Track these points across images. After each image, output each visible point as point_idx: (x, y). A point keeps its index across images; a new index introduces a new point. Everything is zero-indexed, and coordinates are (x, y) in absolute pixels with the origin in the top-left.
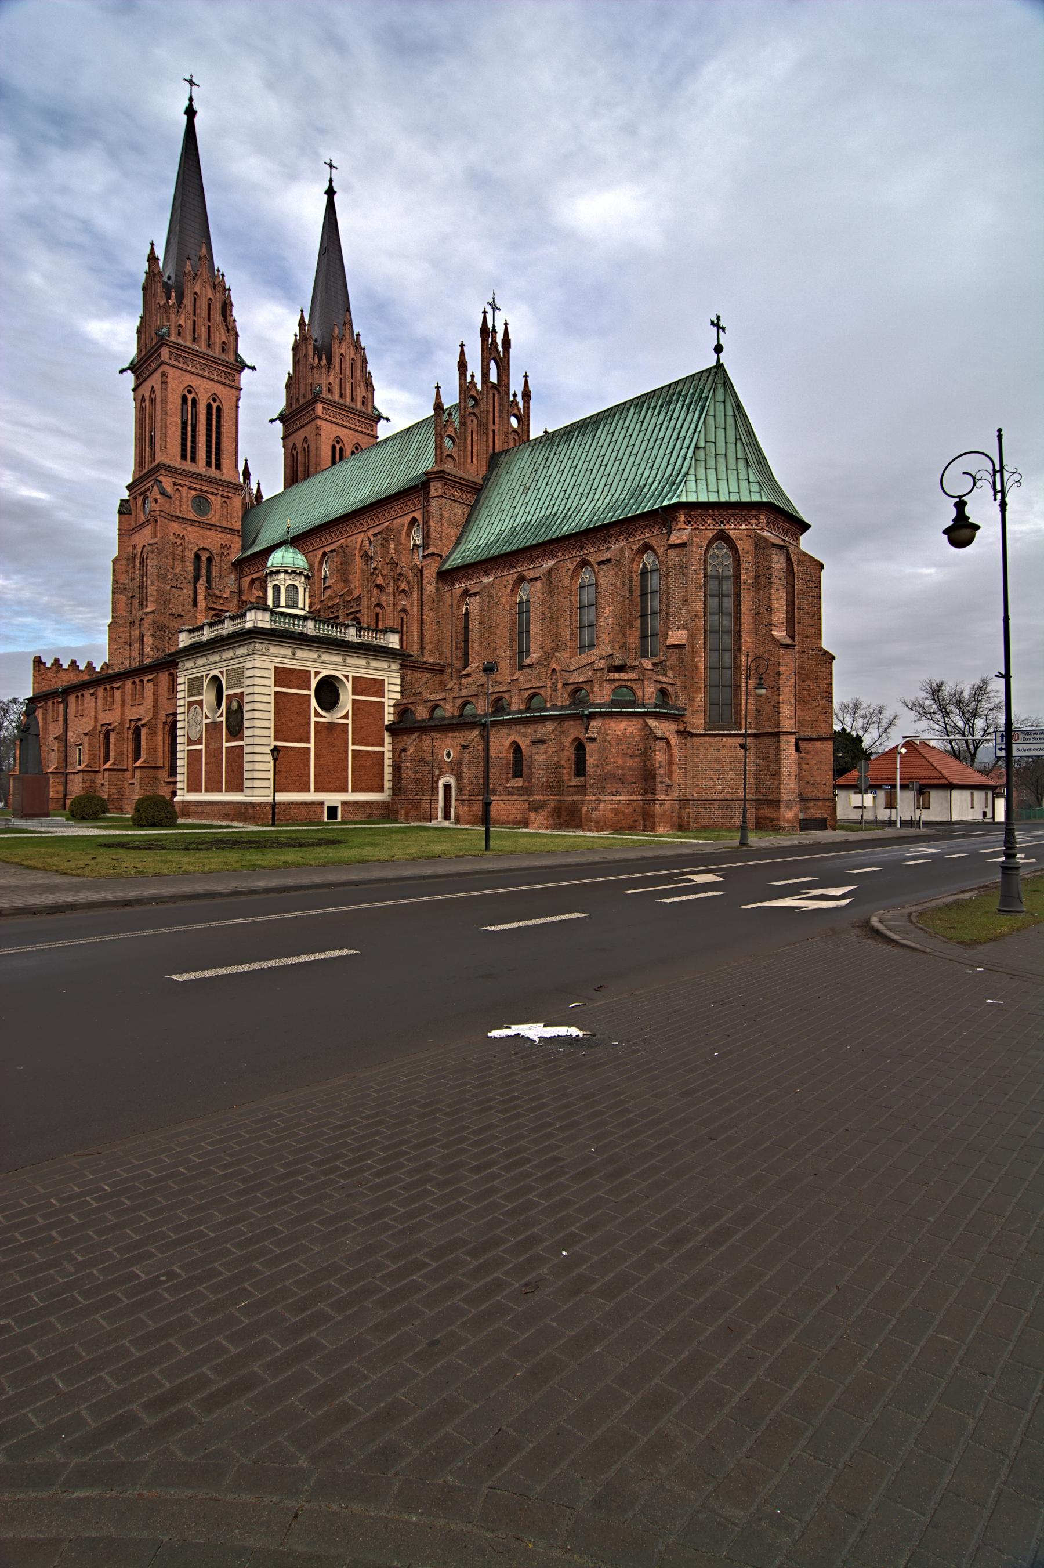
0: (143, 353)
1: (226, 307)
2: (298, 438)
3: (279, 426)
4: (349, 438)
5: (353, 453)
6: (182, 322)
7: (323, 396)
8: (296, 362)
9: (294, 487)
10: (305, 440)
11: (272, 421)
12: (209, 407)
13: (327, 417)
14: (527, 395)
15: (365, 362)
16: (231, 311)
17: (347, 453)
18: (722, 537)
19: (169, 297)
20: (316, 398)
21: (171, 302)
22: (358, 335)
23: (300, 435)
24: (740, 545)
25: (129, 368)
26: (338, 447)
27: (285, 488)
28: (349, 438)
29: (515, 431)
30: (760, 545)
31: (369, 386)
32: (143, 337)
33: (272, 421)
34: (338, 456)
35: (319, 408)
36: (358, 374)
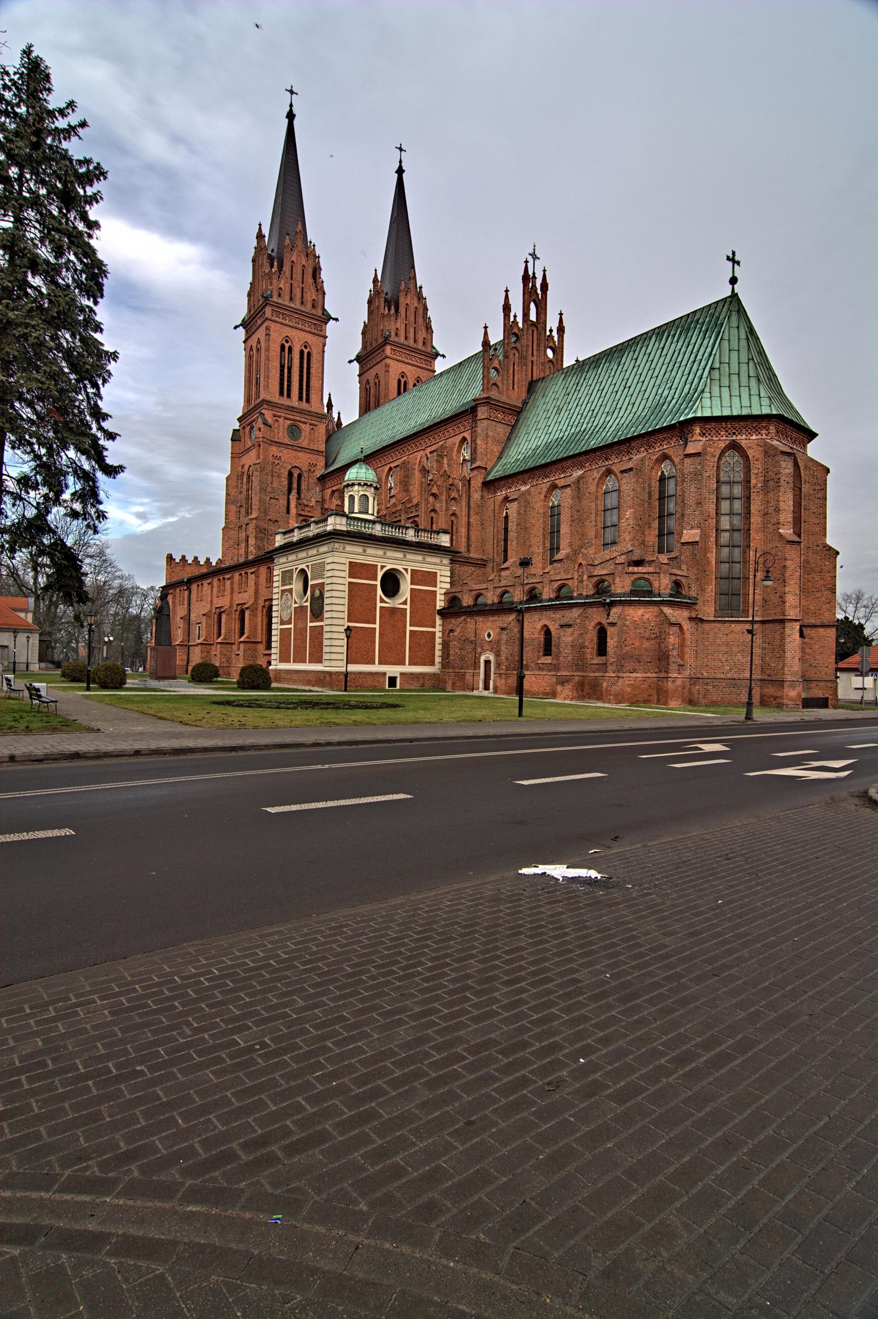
1: (316, 271)
4: (411, 373)
5: (415, 385)
8: (370, 313)
9: (367, 415)
10: (377, 376)
11: (350, 362)
12: (302, 352)
14: (561, 330)
15: (426, 309)
16: (320, 274)
17: (410, 385)
18: (734, 446)
19: (272, 266)
20: (386, 341)
21: (274, 270)
22: (421, 287)
24: (750, 453)
25: (241, 325)
26: (403, 381)
28: (411, 373)
29: (550, 361)
30: (769, 452)
31: (429, 329)
33: (350, 362)
34: (402, 388)
35: (388, 349)
36: (420, 320)
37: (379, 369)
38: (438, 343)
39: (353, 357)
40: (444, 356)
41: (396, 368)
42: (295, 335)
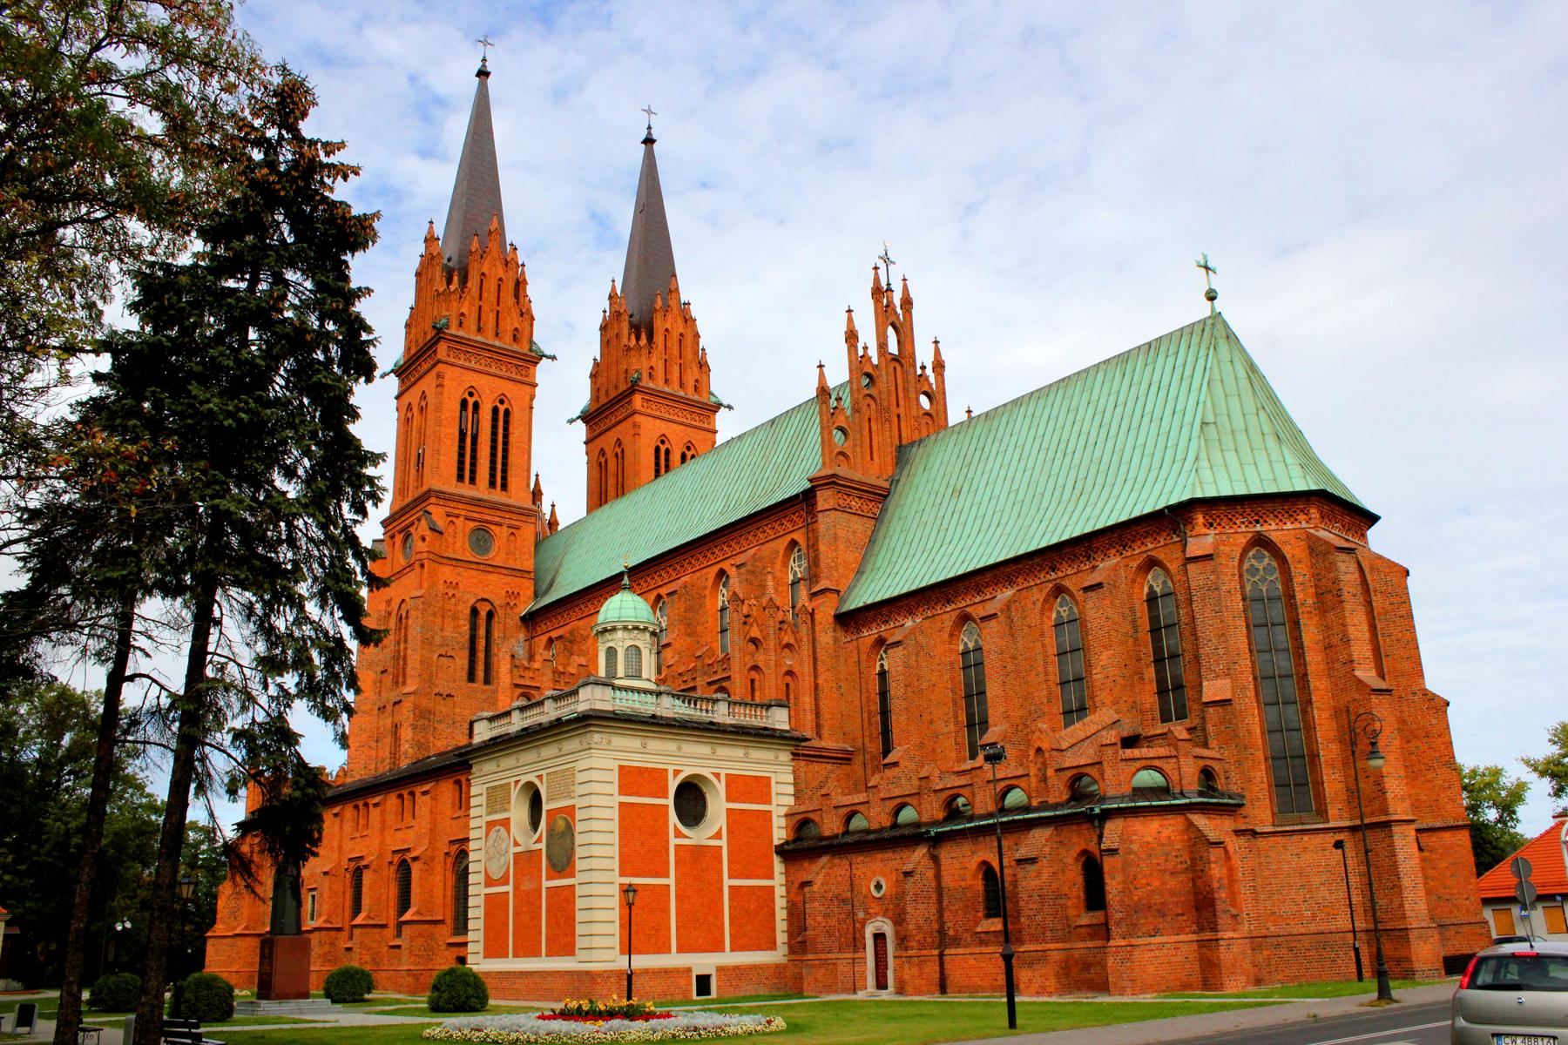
0: (413, 352)
1: (520, 284)
2: (608, 441)
3: (581, 429)
5: (684, 458)
6: (464, 310)
8: (606, 344)
9: (606, 508)
10: (619, 443)
11: (571, 421)
13: (649, 411)
14: (939, 366)
16: (525, 289)
18: (1261, 541)
19: (449, 282)
20: (634, 388)
21: (452, 288)
23: (609, 439)
24: (1288, 551)
25: (392, 371)
27: (590, 510)
28: (678, 437)
29: (927, 414)
30: (1317, 550)
32: (414, 331)
33: (571, 421)
34: (662, 464)
35: (638, 400)
37: (622, 431)
39: (578, 413)
42: (480, 382)
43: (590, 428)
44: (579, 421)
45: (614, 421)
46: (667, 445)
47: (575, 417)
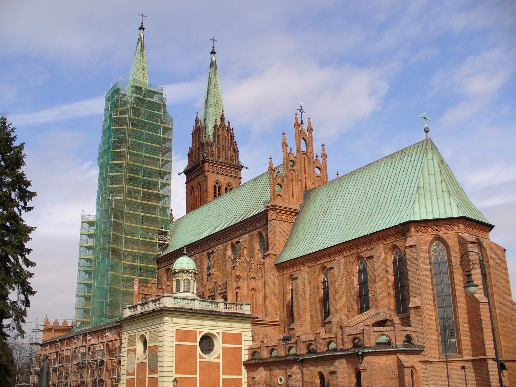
2: (195, 183)
3: (184, 176)
4: (224, 181)
5: (226, 190)
7: (209, 158)
8: (194, 141)
9: (191, 212)
10: (199, 183)
11: (179, 174)
13: (211, 170)
14: (324, 155)
15: (232, 137)
17: (223, 190)
20: (204, 162)
23: (196, 181)
26: (217, 186)
27: (187, 213)
28: (224, 181)
31: (236, 151)
33: (179, 174)
34: (218, 192)
35: (206, 165)
36: (228, 144)
37: (200, 179)
38: (242, 159)
39: (182, 171)
40: (247, 168)
41: (212, 179)
43: (188, 177)
44: (183, 174)
45: (197, 174)
46: (219, 184)
47: (181, 172)
